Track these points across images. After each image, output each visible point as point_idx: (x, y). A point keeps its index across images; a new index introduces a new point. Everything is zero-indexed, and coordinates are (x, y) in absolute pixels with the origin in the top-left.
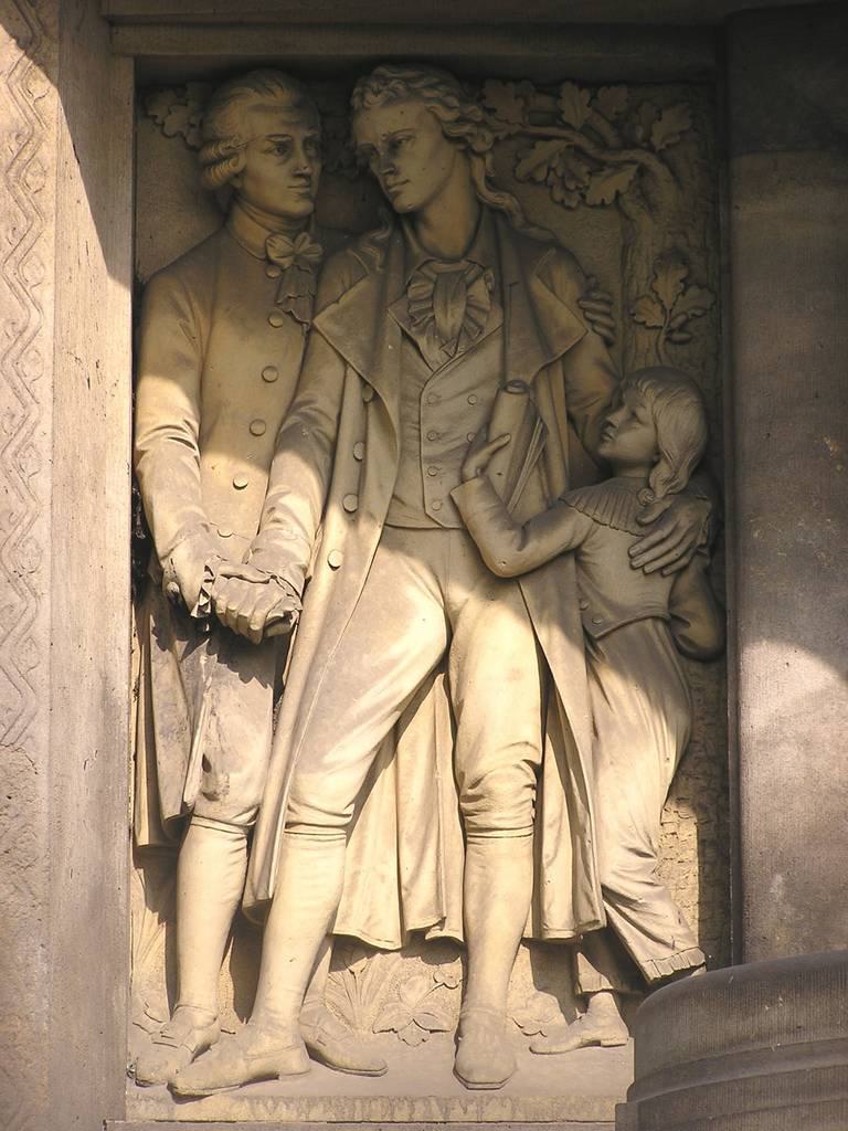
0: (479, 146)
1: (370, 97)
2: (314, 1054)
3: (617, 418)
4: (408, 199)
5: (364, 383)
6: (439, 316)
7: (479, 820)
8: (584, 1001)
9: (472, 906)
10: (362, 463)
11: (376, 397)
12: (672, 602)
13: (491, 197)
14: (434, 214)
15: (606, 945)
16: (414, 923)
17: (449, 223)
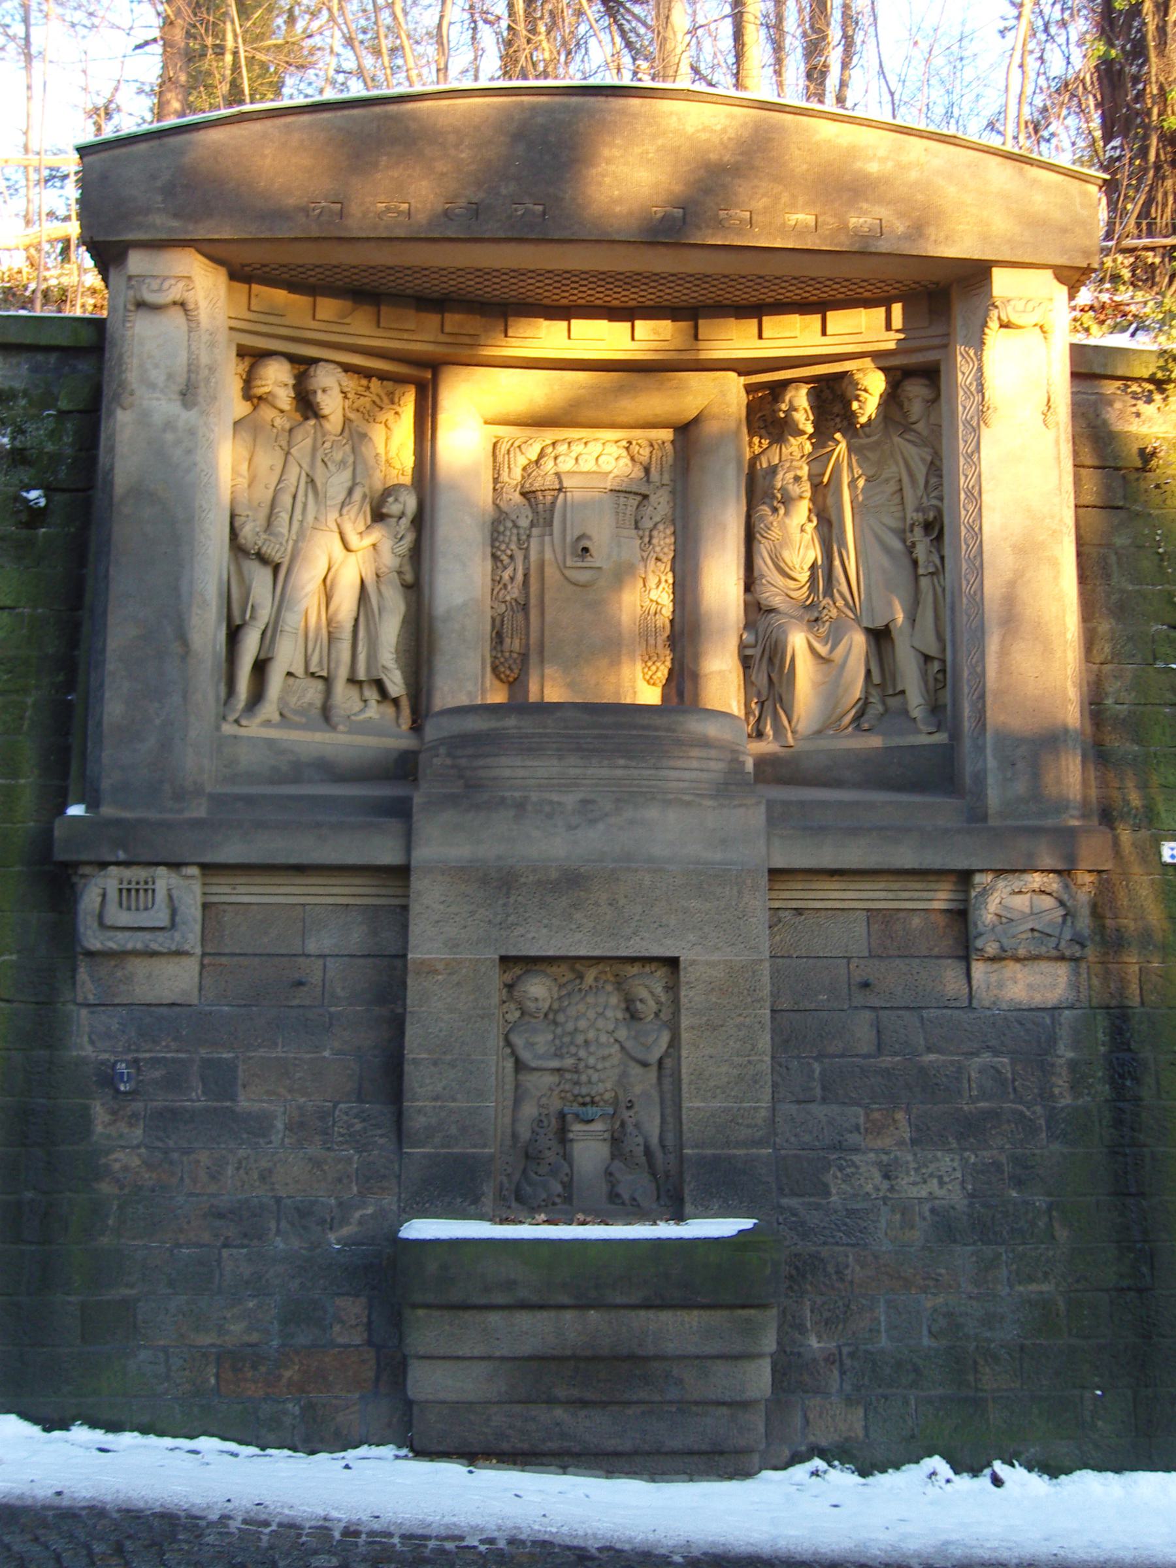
0: (349, 395)
1: (318, 372)
2: (281, 715)
3: (391, 499)
4: (326, 412)
5: (308, 475)
6: (334, 454)
7: (337, 635)
8: (365, 701)
9: (333, 665)
10: (305, 505)
11: (312, 480)
12: (401, 566)
13: (352, 415)
14: (332, 418)
15: (379, 685)
16: (312, 669)
17: (334, 423)
